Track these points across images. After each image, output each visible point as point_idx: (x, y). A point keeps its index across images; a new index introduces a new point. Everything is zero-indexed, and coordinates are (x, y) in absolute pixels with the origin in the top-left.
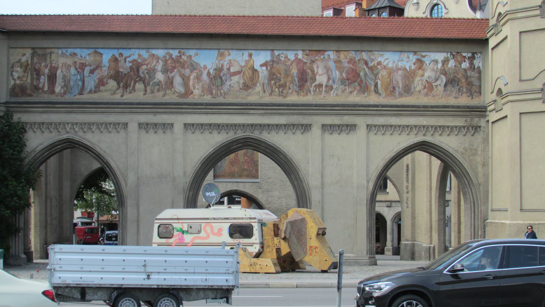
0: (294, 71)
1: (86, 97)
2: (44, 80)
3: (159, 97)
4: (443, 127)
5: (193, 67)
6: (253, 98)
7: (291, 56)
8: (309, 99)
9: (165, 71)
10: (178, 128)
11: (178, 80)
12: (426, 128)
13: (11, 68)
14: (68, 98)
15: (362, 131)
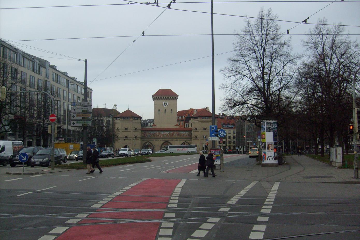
0: (172, 134)
1: (149, 137)
2: (145, 135)
3: (157, 137)
4: (188, 140)
5: (161, 134)
6: (167, 137)
7: (171, 132)
8: (173, 137)
9: (158, 134)
10: (159, 140)
11: (159, 135)
12: (186, 140)
13: (142, 134)
14: (148, 137)
15: (179, 140)
